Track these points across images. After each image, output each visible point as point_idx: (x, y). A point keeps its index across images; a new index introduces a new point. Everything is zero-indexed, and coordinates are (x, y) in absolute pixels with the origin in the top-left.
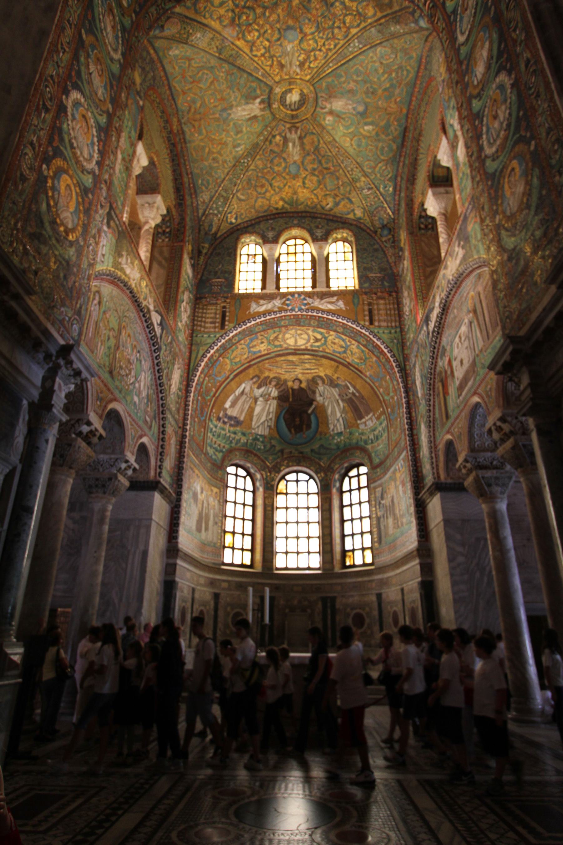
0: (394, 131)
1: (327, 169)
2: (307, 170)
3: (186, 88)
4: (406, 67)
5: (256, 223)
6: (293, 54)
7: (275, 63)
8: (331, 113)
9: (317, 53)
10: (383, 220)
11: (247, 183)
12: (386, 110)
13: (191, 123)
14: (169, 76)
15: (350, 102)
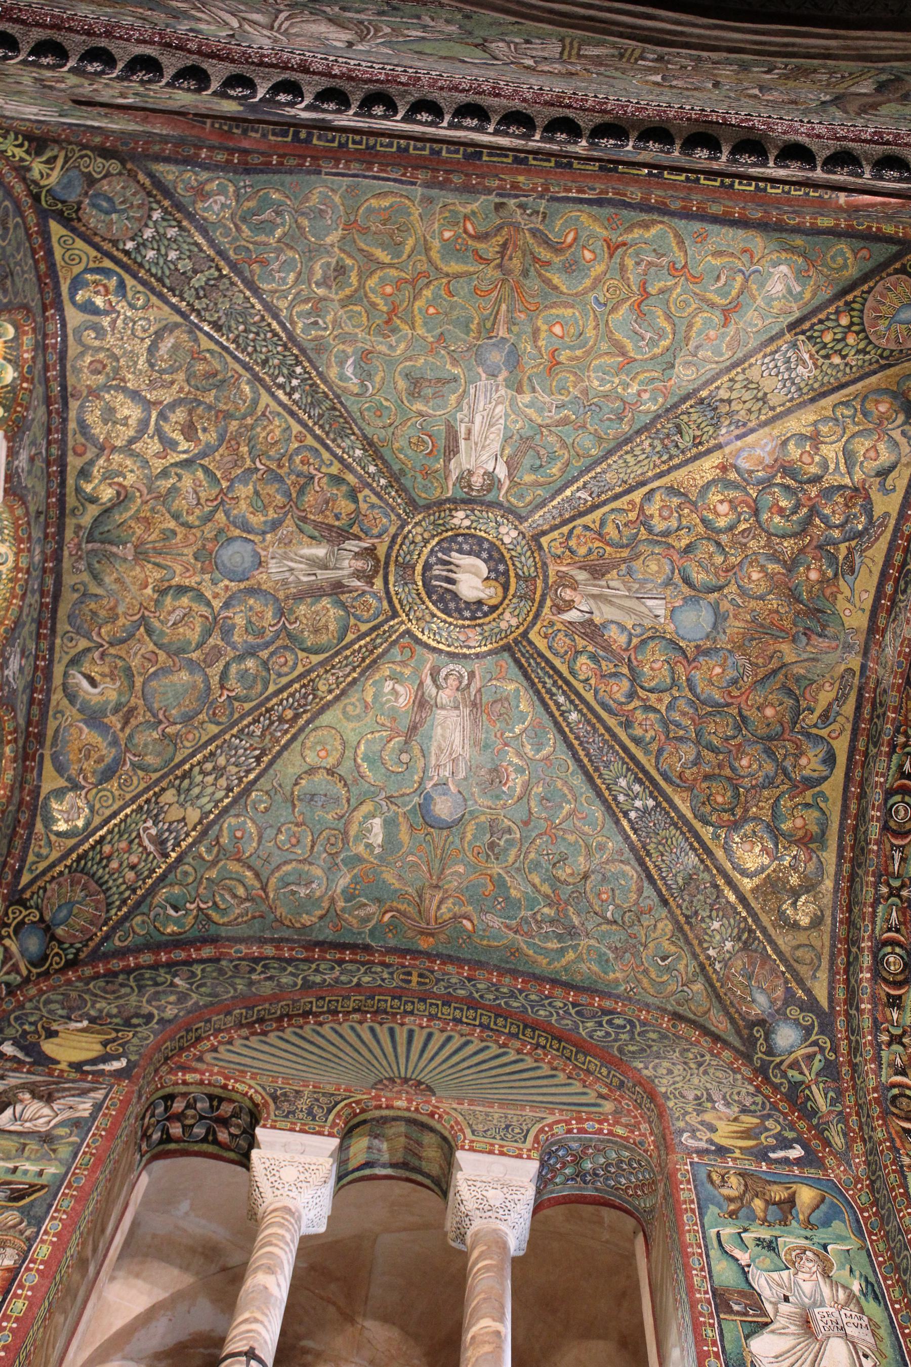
0: (362, 913)
1: (224, 675)
2: (227, 605)
3: (630, 263)
4: (575, 948)
5: (47, 380)
6: (630, 611)
7: (608, 549)
8: (422, 703)
9: (626, 685)
10: (64, 922)
11: (215, 375)
12: (437, 887)
13: (499, 229)
14: (697, 226)
15: (462, 775)
